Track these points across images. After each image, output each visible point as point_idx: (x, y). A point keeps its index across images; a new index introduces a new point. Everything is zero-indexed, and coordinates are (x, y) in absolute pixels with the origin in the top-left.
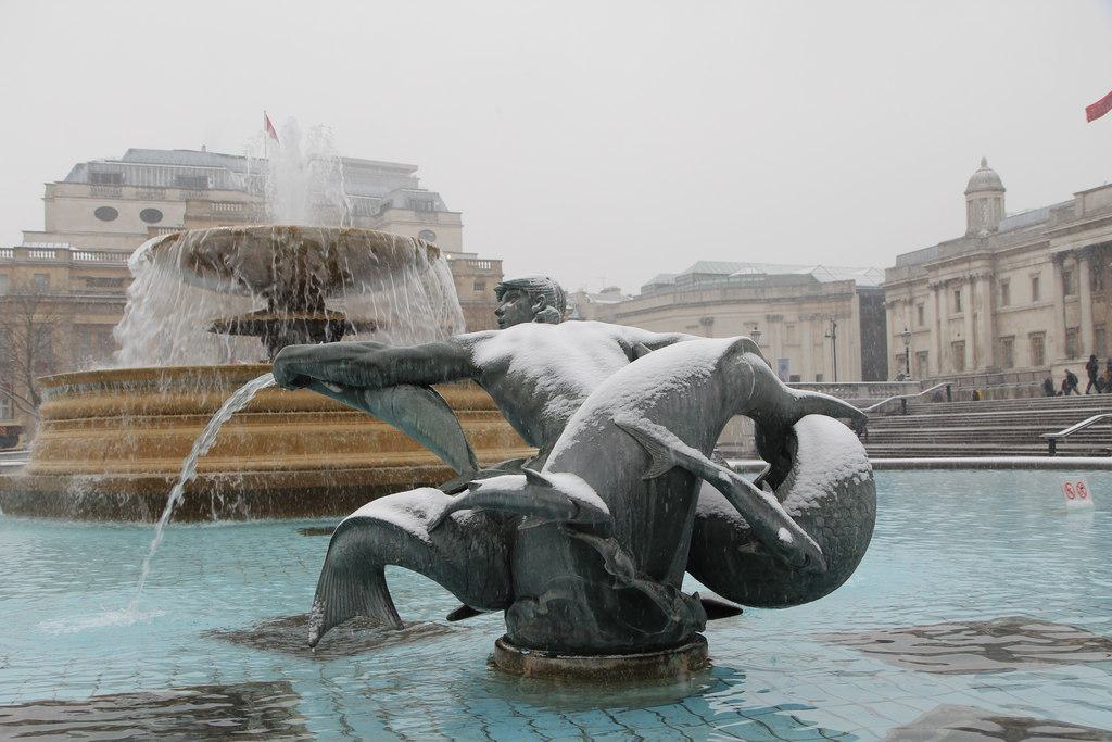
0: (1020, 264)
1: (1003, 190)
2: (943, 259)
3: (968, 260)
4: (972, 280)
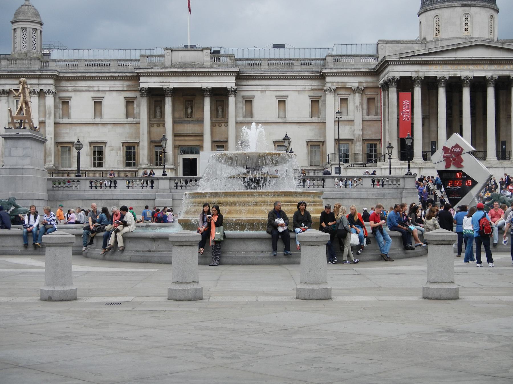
0: (84, 89)
2: (11, 71)
3: (39, 77)
4: (41, 94)
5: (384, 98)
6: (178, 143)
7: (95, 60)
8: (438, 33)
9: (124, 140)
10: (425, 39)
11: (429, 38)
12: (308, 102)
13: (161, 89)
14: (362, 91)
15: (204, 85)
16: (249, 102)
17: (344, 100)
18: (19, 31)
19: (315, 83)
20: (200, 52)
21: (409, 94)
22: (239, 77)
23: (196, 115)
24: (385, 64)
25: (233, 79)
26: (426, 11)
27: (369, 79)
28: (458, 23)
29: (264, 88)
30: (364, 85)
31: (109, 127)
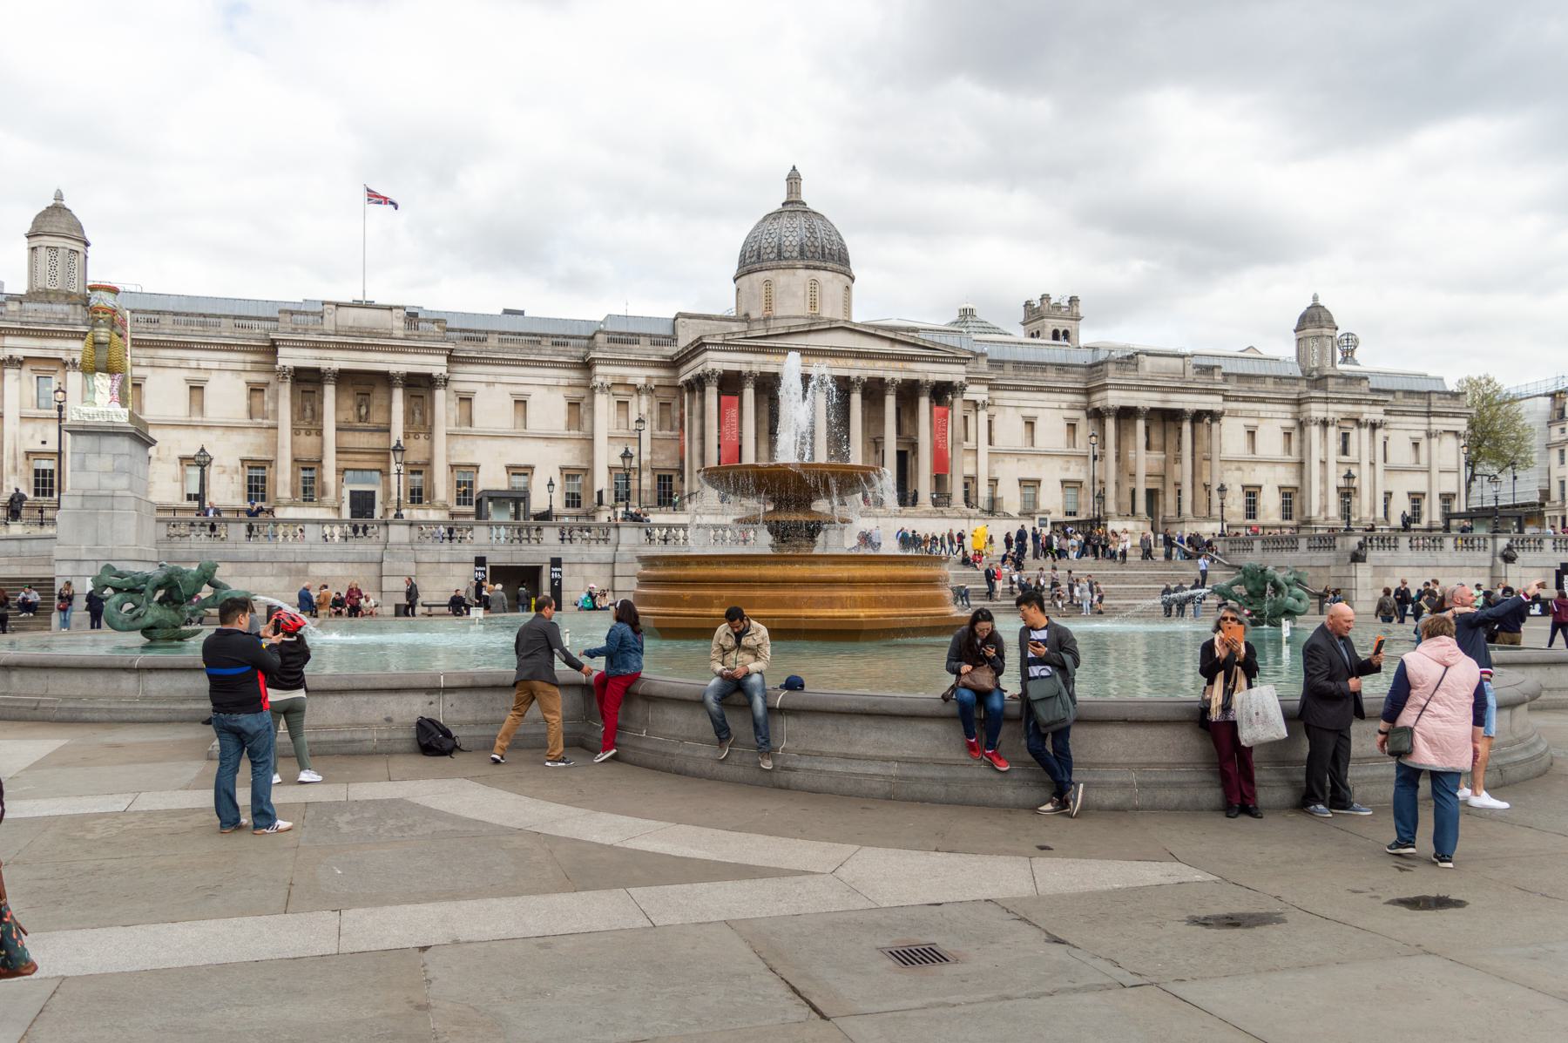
0: (171, 363)
1: (87, 244)
2: (27, 323)
5: (690, 404)
6: (343, 465)
7: (192, 314)
8: (769, 307)
9: (245, 455)
10: (747, 315)
11: (754, 315)
12: (564, 405)
13: (317, 371)
14: (650, 391)
15: (393, 369)
16: (466, 400)
17: (623, 405)
18: (42, 252)
19: (574, 375)
20: (387, 313)
21: (736, 399)
22: (452, 359)
23: (377, 418)
24: (699, 347)
25: (443, 360)
26: (749, 272)
27: (662, 372)
28: (801, 293)
29: (491, 379)
30: (655, 382)
31: (218, 432)
